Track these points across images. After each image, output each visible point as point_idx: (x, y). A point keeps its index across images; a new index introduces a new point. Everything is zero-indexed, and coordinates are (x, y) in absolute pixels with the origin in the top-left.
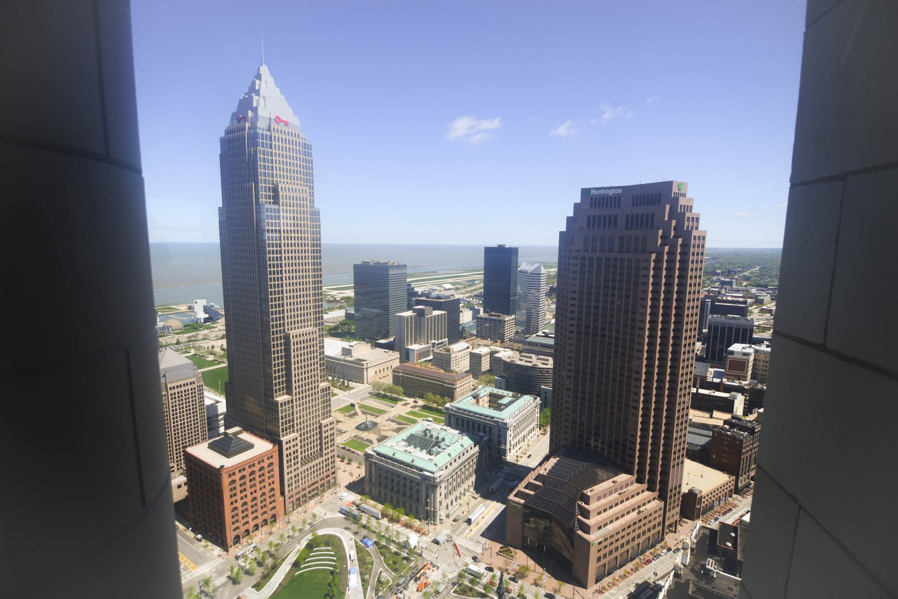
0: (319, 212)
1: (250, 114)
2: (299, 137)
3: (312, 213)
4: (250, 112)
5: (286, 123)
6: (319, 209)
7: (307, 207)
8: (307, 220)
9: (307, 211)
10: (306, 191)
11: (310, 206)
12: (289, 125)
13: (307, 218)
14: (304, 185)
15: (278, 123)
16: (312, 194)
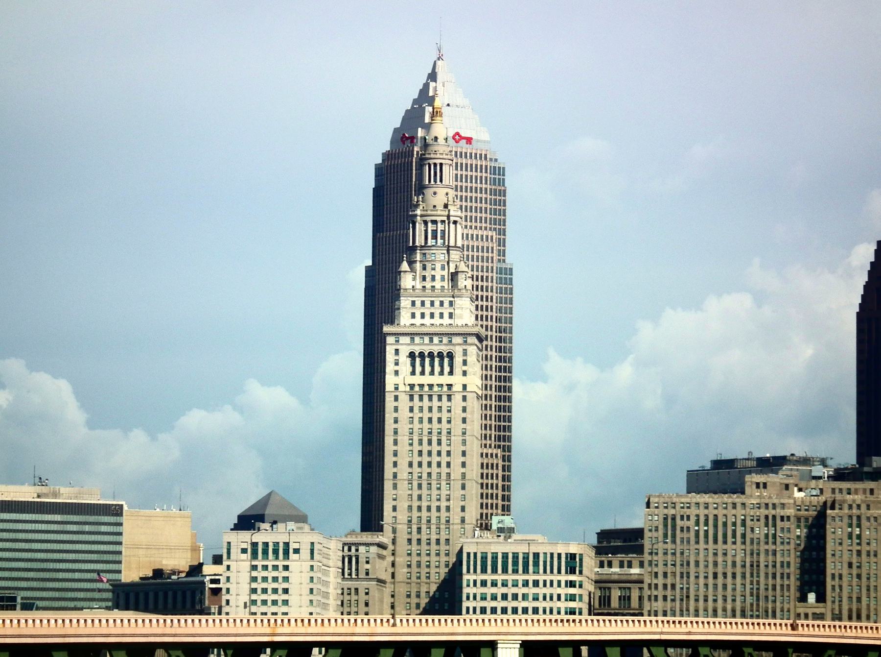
0: (511, 269)
1: (420, 133)
2: (486, 158)
3: (500, 271)
4: (420, 129)
5: (469, 140)
6: (512, 264)
7: (492, 262)
8: (492, 282)
9: (492, 268)
10: (492, 237)
11: (499, 260)
12: (473, 142)
13: (492, 277)
14: (490, 229)
15: (457, 142)
16: (502, 243)
